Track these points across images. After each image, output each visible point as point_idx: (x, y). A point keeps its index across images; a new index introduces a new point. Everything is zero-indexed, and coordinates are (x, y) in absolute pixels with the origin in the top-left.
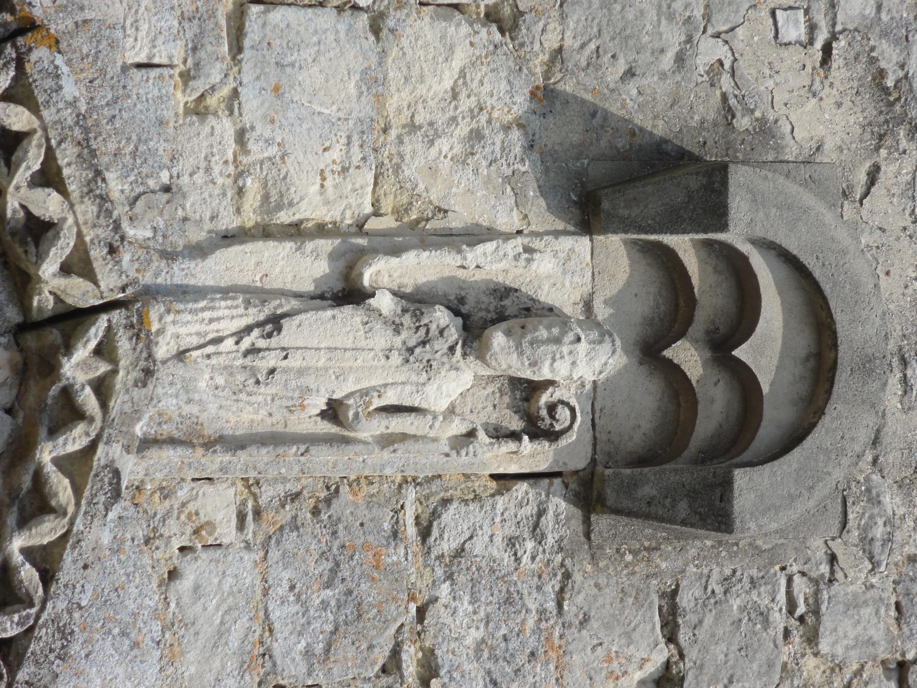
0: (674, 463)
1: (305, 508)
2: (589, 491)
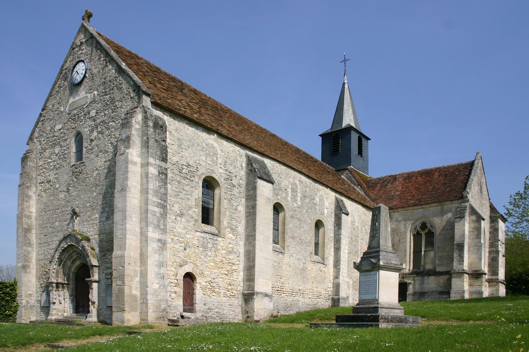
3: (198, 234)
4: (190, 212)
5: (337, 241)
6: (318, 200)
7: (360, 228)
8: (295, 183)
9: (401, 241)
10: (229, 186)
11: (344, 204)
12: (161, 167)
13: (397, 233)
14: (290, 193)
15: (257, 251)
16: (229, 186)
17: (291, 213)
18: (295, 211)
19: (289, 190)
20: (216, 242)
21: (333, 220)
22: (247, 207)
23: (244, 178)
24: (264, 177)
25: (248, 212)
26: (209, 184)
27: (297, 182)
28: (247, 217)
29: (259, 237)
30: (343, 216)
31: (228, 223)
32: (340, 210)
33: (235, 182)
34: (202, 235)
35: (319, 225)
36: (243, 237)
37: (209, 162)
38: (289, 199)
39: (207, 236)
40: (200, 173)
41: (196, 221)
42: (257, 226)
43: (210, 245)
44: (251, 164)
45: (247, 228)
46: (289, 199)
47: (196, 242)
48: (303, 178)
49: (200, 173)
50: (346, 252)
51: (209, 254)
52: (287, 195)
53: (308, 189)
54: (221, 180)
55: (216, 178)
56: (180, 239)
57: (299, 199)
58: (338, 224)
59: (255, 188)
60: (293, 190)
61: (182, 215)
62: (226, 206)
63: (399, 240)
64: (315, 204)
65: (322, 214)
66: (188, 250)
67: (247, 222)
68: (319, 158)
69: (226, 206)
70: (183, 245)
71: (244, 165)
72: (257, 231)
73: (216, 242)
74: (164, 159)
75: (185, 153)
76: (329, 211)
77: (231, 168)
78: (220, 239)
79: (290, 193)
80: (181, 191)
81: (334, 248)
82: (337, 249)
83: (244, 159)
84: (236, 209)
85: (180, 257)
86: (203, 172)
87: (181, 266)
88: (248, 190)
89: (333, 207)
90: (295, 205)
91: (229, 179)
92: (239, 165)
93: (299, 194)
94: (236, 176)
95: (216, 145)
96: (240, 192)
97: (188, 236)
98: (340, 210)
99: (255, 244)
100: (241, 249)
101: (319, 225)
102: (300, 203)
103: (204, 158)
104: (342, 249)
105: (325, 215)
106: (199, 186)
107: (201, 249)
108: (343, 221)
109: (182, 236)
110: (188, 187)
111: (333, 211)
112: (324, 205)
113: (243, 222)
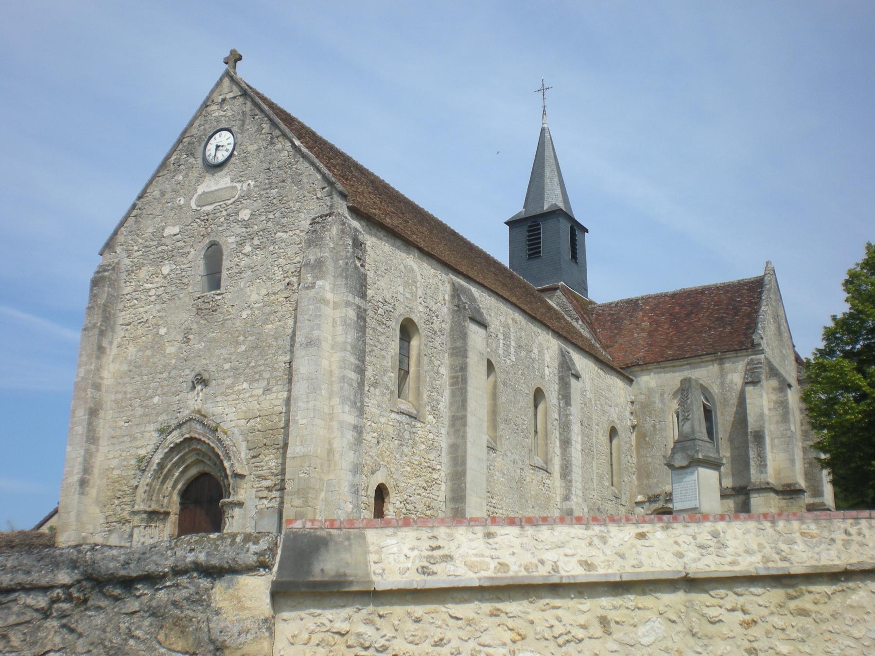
0: (204, 382)
1: (205, 401)
2: (206, 386)
3: (393, 415)
4: (386, 379)
5: (565, 427)
6: (536, 351)
7: (593, 402)
8: (508, 324)
9: (658, 427)
10: (429, 334)
11: (571, 359)
12: (360, 307)
13: (650, 413)
14: (501, 341)
15: (469, 445)
16: (429, 334)
17: (503, 376)
18: (508, 373)
19: (501, 336)
20: (414, 430)
21: (556, 387)
22: (453, 368)
23: (448, 318)
24: (478, 318)
25: (454, 377)
26: (407, 330)
27: (510, 322)
28: (452, 385)
29: (471, 420)
30: (573, 381)
31: (429, 396)
32: (567, 373)
33: (436, 326)
34: (398, 417)
35: (539, 395)
36: (446, 420)
37: (408, 295)
38: (501, 352)
39: (404, 418)
40: (397, 314)
41: (392, 393)
42: (469, 401)
43: (407, 435)
44: (458, 295)
45: (452, 404)
46: (501, 352)
47: (390, 430)
48: (518, 316)
49: (397, 314)
50: (579, 447)
51: (406, 450)
52: (498, 346)
53: (523, 334)
54: (420, 324)
55: (416, 320)
56: (373, 424)
57: (512, 350)
58: (566, 397)
59: (464, 336)
60: (506, 337)
61: (375, 385)
62: (426, 368)
63: (654, 426)
64: (533, 360)
65: (542, 377)
66: (381, 445)
67: (453, 394)
68: (506, 264)
69: (426, 368)
70: (375, 435)
71: (447, 297)
72: (469, 409)
73: (414, 430)
74: (363, 296)
75: (382, 283)
76: (551, 370)
77: (431, 304)
78: (419, 425)
79: (501, 341)
80: (377, 344)
81: (560, 440)
82: (566, 443)
83: (448, 287)
84: (438, 373)
85: (372, 457)
86: (401, 312)
87: (373, 472)
88: (453, 340)
89: (556, 364)
90: (508, 361)
91: (429, 322)
92: (441, 298)
93: (513, 343)
94: (437, 316)
95: (415, 267)
96: (442, 342)
97: (383, 420)
98: (567, 373)
99: (465, 432)
100: (444, 442)
101: (539, 395)
102: (514, 359)
103: (401, 289)
104: (573, 442)
105: (547, 379)
106: (396, 336)
107: (396, 442)
108: (573, 390)
109: (376, 420)
110: (384, 337)
111: (556, 371)
112: (544, 360)
113: (447, 394)
